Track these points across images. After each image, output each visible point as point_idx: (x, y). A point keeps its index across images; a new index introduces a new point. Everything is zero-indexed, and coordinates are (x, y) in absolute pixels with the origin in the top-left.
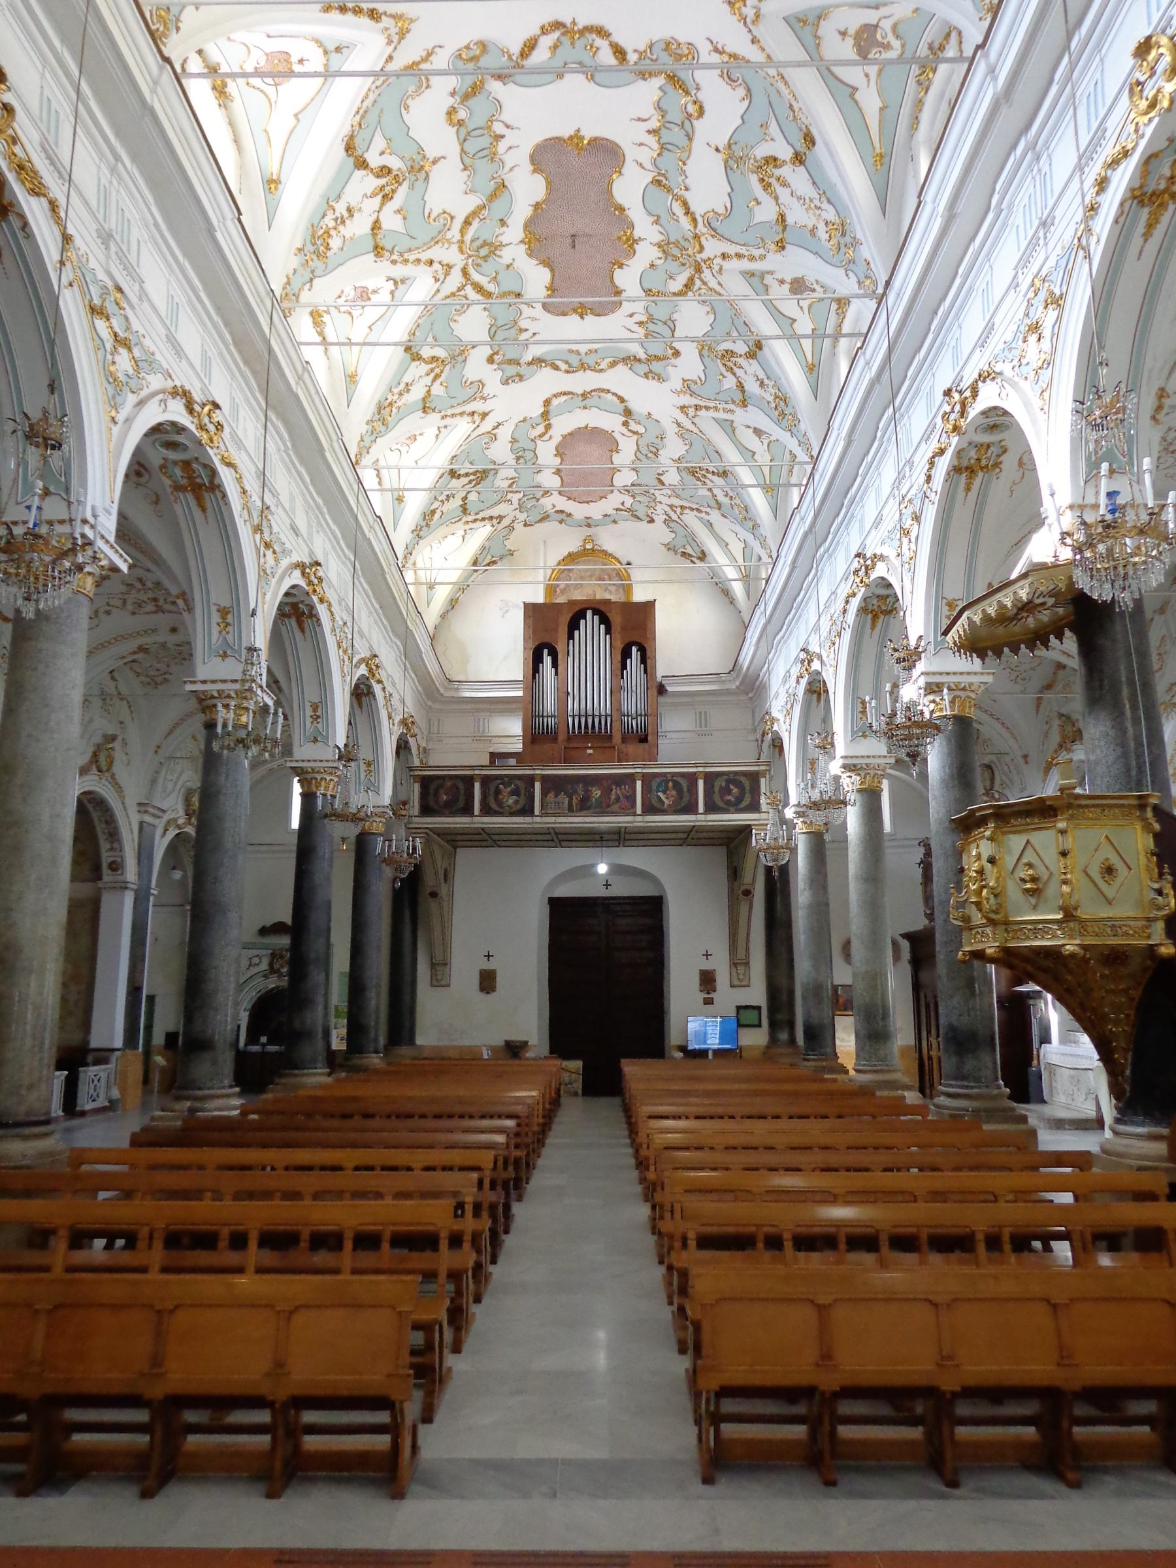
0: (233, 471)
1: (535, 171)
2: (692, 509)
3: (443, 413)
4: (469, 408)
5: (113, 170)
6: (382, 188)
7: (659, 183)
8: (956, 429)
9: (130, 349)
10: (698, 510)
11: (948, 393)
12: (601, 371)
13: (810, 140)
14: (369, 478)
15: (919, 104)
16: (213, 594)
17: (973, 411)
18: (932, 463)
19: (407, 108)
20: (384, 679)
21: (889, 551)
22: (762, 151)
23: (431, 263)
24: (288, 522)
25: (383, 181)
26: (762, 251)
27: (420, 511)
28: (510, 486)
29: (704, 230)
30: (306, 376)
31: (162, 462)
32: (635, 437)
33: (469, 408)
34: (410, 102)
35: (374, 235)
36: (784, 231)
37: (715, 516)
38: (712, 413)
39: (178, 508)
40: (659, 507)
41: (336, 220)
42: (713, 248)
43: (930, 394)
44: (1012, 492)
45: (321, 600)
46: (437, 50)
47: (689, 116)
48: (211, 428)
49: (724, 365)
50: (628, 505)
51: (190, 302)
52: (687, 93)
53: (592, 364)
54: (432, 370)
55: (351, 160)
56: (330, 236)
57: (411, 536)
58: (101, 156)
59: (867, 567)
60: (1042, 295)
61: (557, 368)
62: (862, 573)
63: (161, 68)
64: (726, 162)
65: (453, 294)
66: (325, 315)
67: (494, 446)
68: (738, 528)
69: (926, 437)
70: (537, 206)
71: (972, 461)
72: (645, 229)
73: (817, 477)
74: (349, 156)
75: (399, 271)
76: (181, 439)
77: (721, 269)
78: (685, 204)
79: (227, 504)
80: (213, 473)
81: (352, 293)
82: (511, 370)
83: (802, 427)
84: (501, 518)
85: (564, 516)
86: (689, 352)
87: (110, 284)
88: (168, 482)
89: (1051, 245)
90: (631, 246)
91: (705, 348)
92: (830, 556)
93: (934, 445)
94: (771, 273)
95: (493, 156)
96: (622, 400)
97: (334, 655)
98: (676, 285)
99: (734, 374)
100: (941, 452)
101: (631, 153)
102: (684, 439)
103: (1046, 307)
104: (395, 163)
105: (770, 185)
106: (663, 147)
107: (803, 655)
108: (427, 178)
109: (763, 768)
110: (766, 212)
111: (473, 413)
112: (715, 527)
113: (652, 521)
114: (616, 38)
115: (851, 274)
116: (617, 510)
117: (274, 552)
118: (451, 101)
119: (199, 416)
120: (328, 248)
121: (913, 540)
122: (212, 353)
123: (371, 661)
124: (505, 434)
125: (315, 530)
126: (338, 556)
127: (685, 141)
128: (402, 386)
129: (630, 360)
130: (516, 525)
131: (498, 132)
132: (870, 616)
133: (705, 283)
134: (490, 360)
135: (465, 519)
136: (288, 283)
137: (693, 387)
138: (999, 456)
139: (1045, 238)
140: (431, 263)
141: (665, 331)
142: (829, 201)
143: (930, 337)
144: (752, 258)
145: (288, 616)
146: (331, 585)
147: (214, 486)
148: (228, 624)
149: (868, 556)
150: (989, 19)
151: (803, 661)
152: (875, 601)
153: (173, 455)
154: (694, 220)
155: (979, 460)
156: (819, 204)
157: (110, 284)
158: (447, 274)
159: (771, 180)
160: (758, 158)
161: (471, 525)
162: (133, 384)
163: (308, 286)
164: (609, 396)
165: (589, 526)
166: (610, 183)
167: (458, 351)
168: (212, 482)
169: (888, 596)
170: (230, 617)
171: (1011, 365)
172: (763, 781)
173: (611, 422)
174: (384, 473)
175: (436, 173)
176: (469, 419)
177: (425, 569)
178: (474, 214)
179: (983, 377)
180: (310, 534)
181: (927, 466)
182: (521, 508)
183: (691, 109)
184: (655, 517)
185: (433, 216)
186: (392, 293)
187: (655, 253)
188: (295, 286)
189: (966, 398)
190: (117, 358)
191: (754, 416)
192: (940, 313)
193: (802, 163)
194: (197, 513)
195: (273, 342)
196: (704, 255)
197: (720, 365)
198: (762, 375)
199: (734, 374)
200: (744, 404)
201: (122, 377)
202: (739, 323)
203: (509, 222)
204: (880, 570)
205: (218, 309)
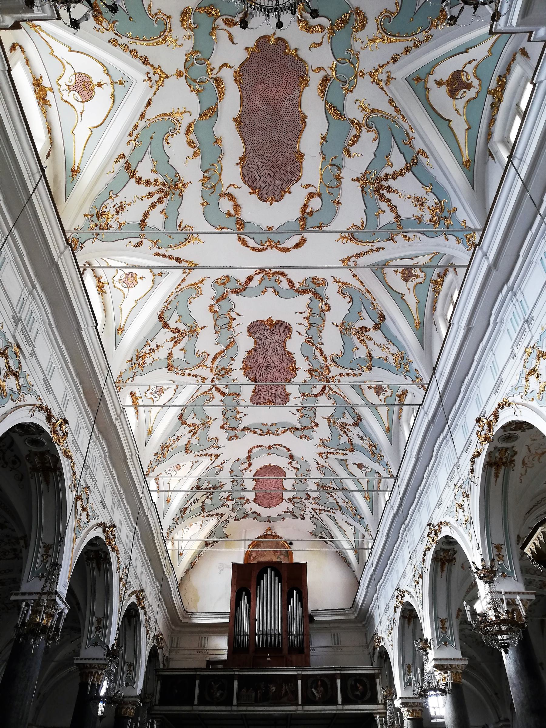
0: (70, 461)
1: (249, 336)
2: (325, 511)
3: (196, 454)
4: (210, 452)
5: (30, 293)
6: (175, 338)
7: (309, 341)
8: (486, 439)
9: (17, 378)
10: (329, 511)
11: (478, 420)
12: (278, 435)
13: (382, 317)
14: (153, 485)
15: (435, 300)
16: (42, 536)
17: (497, 428)
18: (473, 462)
19: (190, 303)
20: (147, 606)
21: (450, 519)
22: (358, 325)
23: (196, 376)
24: (100, 499)
25: (175, 335)
26: (360, 371)
27: (179, 508)
28: (229, 496)
29: (331, 363)
30: (122, 416)
31: (28, 453)
32: (295, 470)
33: (210, 452)
34: (191, 300)
35: (169, 359)
36: (371, 361)
37: (338, 514)
38: (336, 456)
39: (32, 481)
40: (307, 510)
41: (150, 350)
42: (335, 371)
43: (465, 427)
44: (521, 480)
45: (113, 549)
46: (206, 278)
47: (323, 311)
48: (61, 434)
49: (342, 430)
50: (290, 509)
51: (62, 367)
52: (322, 300)
53: (274, 431)
54: (192, 430)
55: (161, 323)
56: (146, 357)
57: (172, 522)
58: (25, 284)
59: (436, 531)
60: (534, 354)
61: (256, 433)
62: (433, 535)
63: (66, 248)
64: (341, 331)
65: (206, 392)
66: (139, 399)
67: (222, 474)
68: (351, 521)
69: (466, 449)
70: (250, 352)
71: (497, 459)
72: (301, 363)
73: (399, 480)
74: (160, 321)
75: (180, 379)
76: (41, 438)
77: (339, 382)
78: (321, 351)
79: (63, 479)
80: (58, 460)
81: (155, 389)
82: (233, 433)
83: (386, 459)
84: (222, 515)
85: (256, 515)
86: (324, 425)
87: (13, 343)
88: (29, 465)
89: (533, 331)
90: (295, 372)
91: (331, 421)
92: (409, 529)
93: (472, 451)
94: (364, 382)
95: (230, 328)
96: (288, 450)
97: (116, 585)
98: (316, 391)
99: (347, 435)
100: (478, 454)
101: (295, 328)
102: (321, 471)
103: (538, 360)
104: (182, 327)
105: (363, 340)
106: (311, 325)
107: (397, 593)
108: (197, 335)
109: (377, 671)
110: (362, 352)
111: (211, 455)
112: (337, 521)
113: (303, 518)
114: (289, 277)
115: (408, 378)
116: (285, 512)
117: (88, 514)
118: (212, 302)
119: (54, 424)
120: (144, 362)
121: (466, 509)
122: (70, 396)
123: (139, 593)
124: (227, 467)
125: (116, 508)
126: (129, 526)
127: (321, 322)
128: (175, 437)
129: (293, 429)
130: (230, 520)
131: (233, 317)
132: (440, 563)
133: (331, 389)
134: (222, 427)
135: (203, 514)
136: (121, 376)
137: (326, 443)
138: (513, 456)
139: (529, 328)
140: (196, 376)
141: (311, 413)
142: (394, 345)
143: (461, 395)
144: (355, 375)
145: (92, 559)
146: (120, 541)
147: (57, 469)
148: (49, 556)
149: (435, 525)
150: (473, 249)
151: (397, 597)
152: (442, 554)
153: (35, 449)
154: (326, 358)
155: (501, 459)
156: (388, 347)
157: (13, 343)
158: (204, 382)
159: (363, 338)
160: (357, 328)
161: (206, 518)
162: (15, 397)
163: (131, 379)
164: (282, 448)
165: (269, 521)
166: (285, 342)
167: (206, 421)
168: (55, 466)
169: (449, 550)
170: (50, 551)
171: (520, 396)
172: (378, 680)
173: (282, 462)
174: (161, 481)
175: (202, 333)
176: (209, 458)
177: (178, 540)
178: (219, 354)
179: (502, 406)
180: (113, 509)
181: (470, 463)
182: (233, 510)
183: (324, 307)
184: (305, 516)
185: (199, 353)
186: (175, 390)
187: (306, 375)
188: (125, 378)
189: (491, 421)
190: (7, 380)
191: (358, 457)
192: (466, 381)
193: (379, 328)
194: (43, 485)
195: (104, 392)
196: (330, 375)
197: (339, 430)
198: (362, 434)
199: (347, 435)
200: (353, 450)
201: (7, 390)
202: (350, 407)
203: (235, 359)
204: (445, 532)
205: (78, 374)
